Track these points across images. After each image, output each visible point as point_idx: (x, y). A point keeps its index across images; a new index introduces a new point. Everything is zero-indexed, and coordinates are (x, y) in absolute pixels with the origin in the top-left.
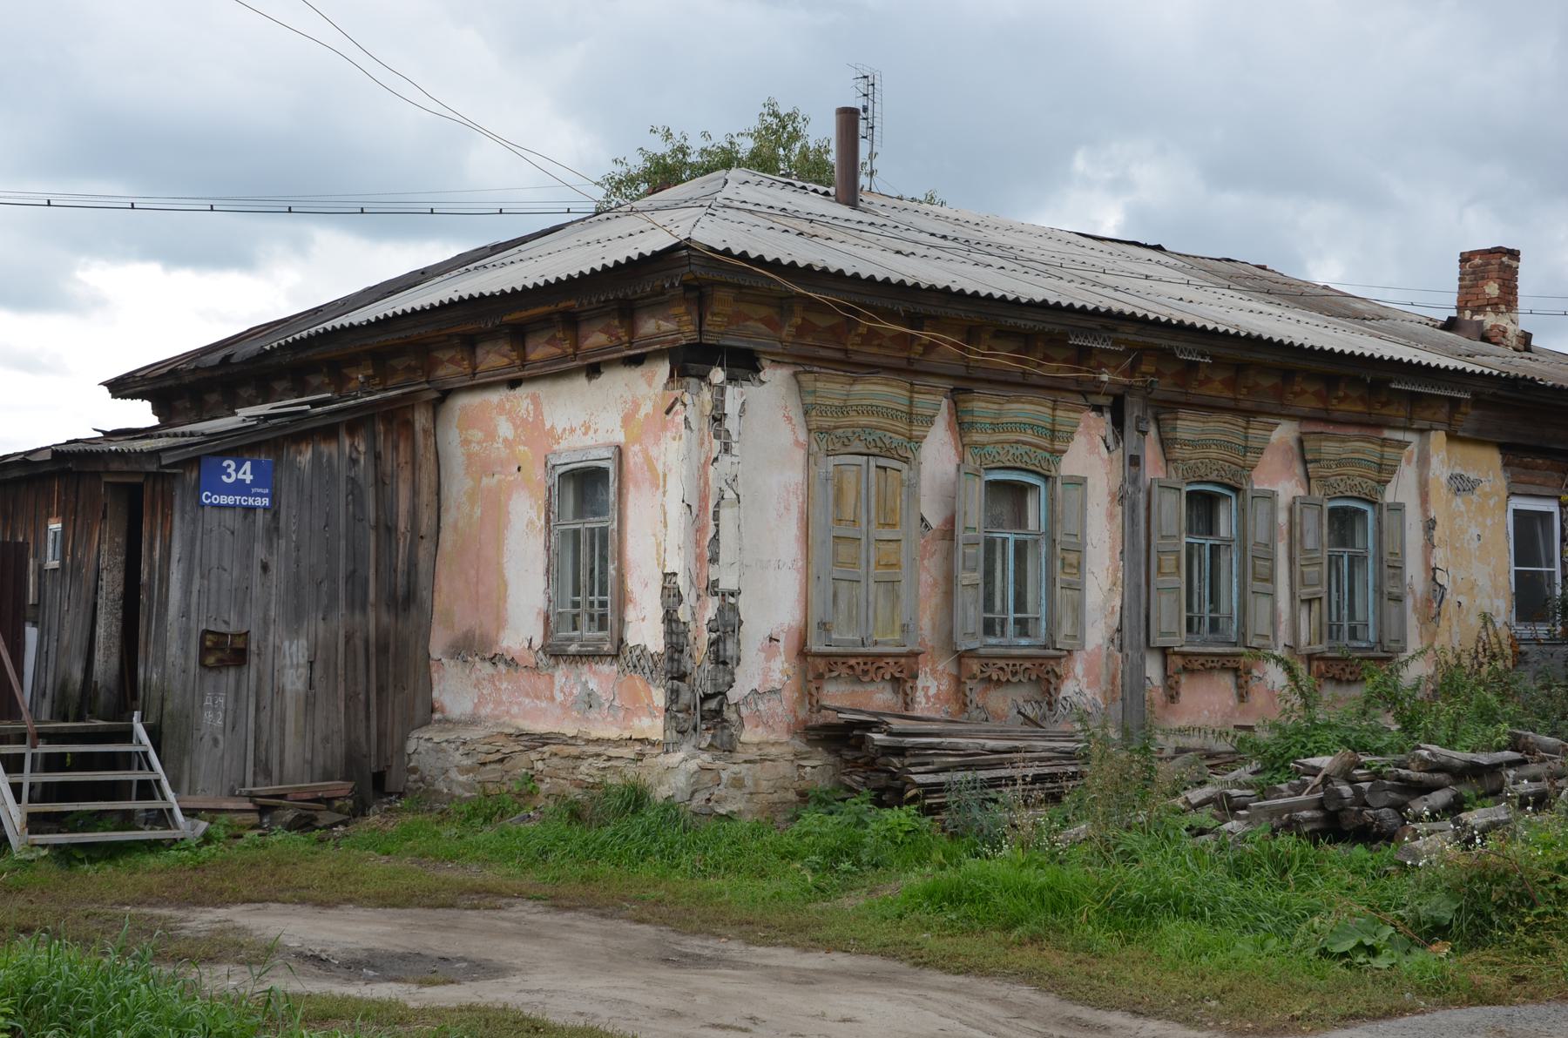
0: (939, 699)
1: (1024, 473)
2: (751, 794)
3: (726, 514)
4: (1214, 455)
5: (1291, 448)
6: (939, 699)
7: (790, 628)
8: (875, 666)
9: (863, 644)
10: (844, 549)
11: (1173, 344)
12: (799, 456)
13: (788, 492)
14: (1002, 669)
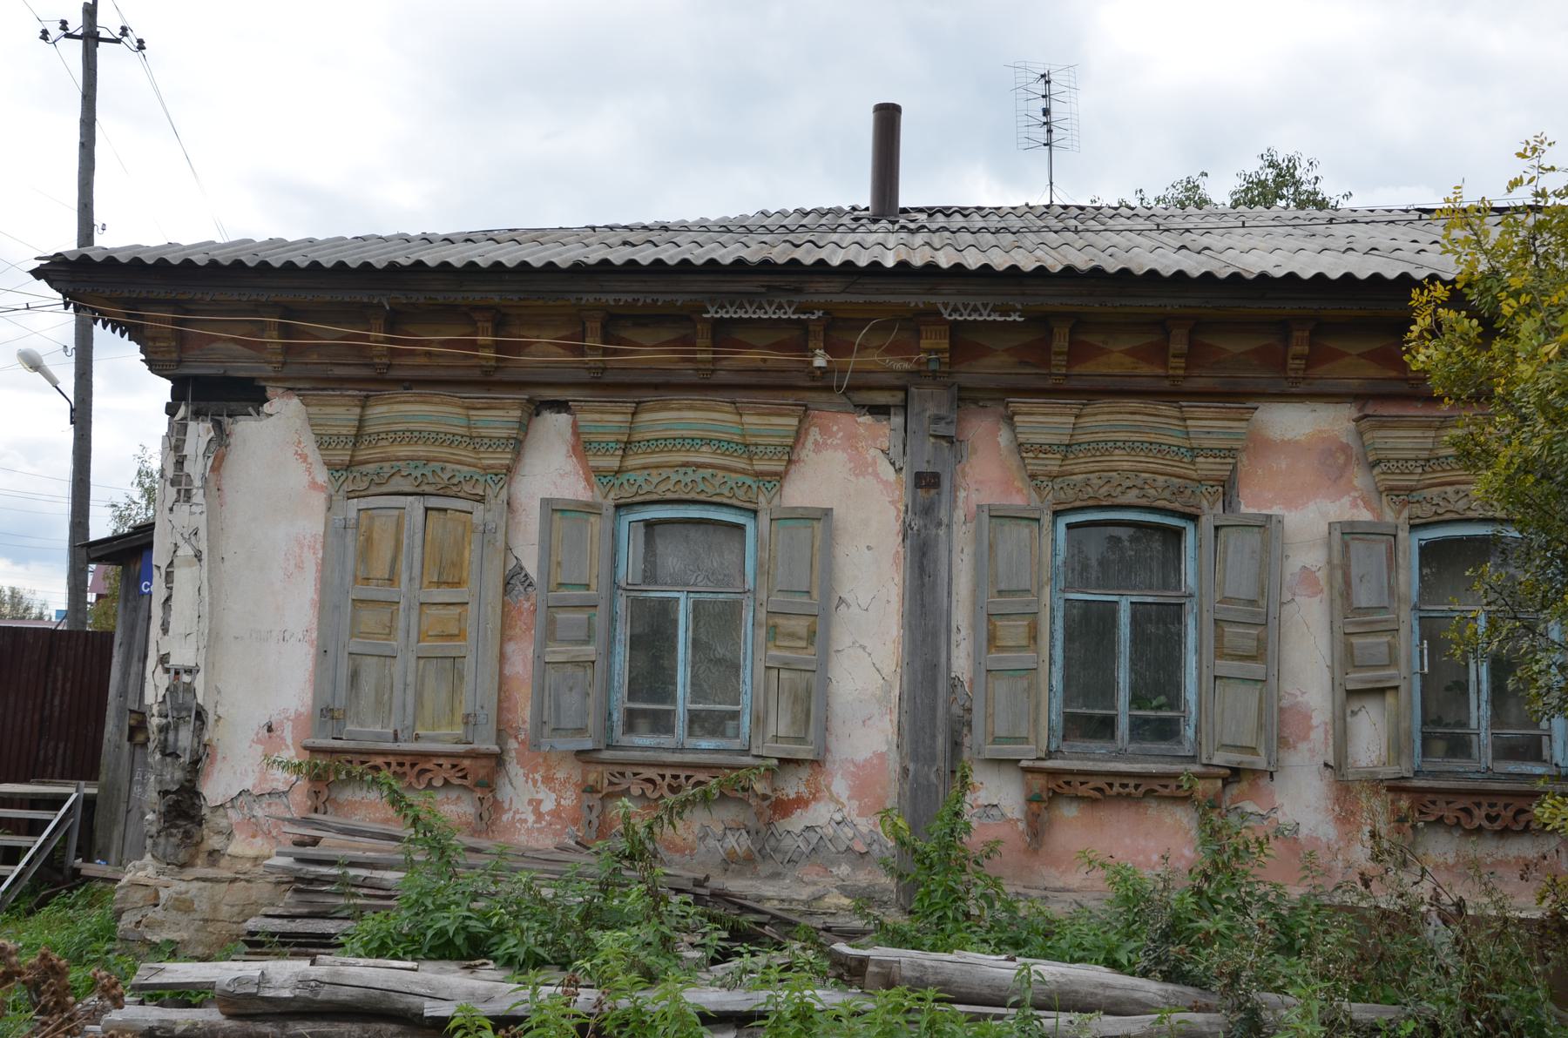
0: (560, 817)
1: (713, 508)
2: (206, 920)
3: (180, 574)
4: (1126, 465)
5: (1344, 448)
6: (560, 817)
7: (298, 715)
8: (417, 769)
9: (396, 739)
10: (370, 619)
11: (933, 299)
12: (319, 500)
13: (302, 548)
14: (650, 781)
